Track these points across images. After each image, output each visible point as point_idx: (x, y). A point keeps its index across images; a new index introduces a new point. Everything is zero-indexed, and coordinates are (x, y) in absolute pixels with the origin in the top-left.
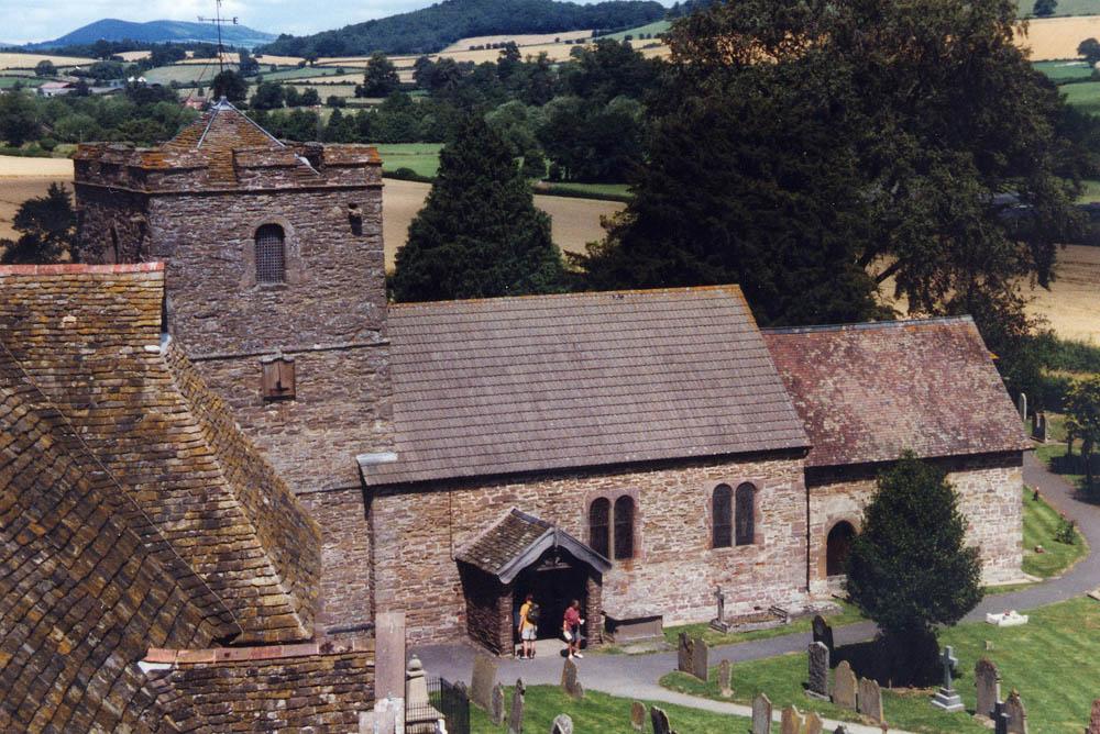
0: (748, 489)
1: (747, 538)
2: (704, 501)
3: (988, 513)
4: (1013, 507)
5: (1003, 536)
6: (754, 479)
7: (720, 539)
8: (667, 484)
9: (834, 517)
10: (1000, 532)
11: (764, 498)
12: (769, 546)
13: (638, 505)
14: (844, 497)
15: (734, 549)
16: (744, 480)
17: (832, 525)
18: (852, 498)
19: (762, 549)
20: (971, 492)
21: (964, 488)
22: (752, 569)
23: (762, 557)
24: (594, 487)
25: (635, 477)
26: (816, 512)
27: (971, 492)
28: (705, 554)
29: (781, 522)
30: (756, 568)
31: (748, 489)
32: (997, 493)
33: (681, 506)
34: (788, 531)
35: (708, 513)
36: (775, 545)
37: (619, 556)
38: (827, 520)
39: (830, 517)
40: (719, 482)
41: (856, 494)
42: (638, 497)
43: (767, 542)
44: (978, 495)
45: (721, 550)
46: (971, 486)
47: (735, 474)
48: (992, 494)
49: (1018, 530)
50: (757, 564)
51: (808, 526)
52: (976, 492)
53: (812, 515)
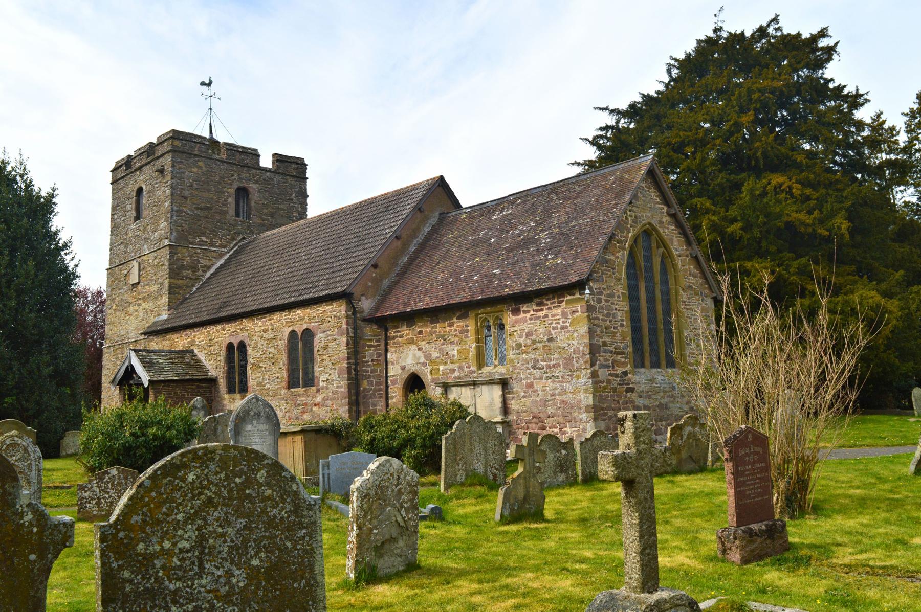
0: (308, 334)
1: (310, 382)
2: (283, 344)
3: (549, 367)
4: (582, 362)
5: (568, 397)
6: (313, 325)
7: (292, 383)
8: (894, 457)
9: (407, 368)
10: (564, 392)
11: (319, 340)
12: (322, 388)
13: (248, 348)
14: (414, 347)
15: (300, 390)
16: (305, 327)
17: (405, 376)
18: (420, 349)
19: (318, 391)
20: (529, 342)
21: (521, 337)
22: (311, 410)
23: (319, 399)
24: (224, 334)
25: (247, 323)
26: (393, 363)
27: (529, 342)
28: (284, 391)
29: (330, 366)
30: (315, 408)
31: (308, 334)
32: (560, 343)
33: (270, 350)
34: (335, 376)
35: (285, 358)
36: (327, 388)
37: (239, 393)
38: (400, 371)
39: (403, 368)
40: (291, 329)
41: (423, 344)
42: (247, 342)
43: (321, 384)
44: (538, 345)
45: (293, 390)
46: (528, 335)
47: (301, 319)
48: (552, 344)
49: (586, 391)
50: (315, 405)
51: (387, 377)
52: (534, 342)
53: (390, 366)
